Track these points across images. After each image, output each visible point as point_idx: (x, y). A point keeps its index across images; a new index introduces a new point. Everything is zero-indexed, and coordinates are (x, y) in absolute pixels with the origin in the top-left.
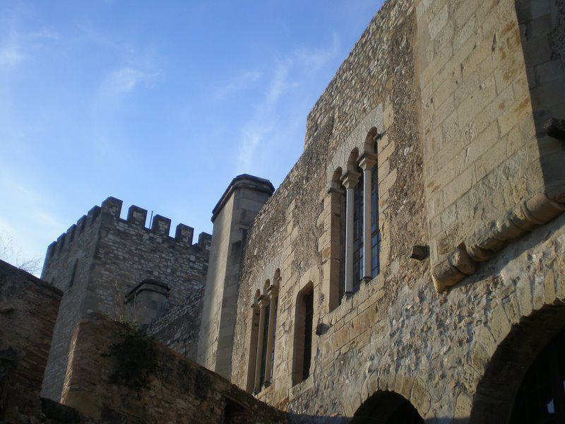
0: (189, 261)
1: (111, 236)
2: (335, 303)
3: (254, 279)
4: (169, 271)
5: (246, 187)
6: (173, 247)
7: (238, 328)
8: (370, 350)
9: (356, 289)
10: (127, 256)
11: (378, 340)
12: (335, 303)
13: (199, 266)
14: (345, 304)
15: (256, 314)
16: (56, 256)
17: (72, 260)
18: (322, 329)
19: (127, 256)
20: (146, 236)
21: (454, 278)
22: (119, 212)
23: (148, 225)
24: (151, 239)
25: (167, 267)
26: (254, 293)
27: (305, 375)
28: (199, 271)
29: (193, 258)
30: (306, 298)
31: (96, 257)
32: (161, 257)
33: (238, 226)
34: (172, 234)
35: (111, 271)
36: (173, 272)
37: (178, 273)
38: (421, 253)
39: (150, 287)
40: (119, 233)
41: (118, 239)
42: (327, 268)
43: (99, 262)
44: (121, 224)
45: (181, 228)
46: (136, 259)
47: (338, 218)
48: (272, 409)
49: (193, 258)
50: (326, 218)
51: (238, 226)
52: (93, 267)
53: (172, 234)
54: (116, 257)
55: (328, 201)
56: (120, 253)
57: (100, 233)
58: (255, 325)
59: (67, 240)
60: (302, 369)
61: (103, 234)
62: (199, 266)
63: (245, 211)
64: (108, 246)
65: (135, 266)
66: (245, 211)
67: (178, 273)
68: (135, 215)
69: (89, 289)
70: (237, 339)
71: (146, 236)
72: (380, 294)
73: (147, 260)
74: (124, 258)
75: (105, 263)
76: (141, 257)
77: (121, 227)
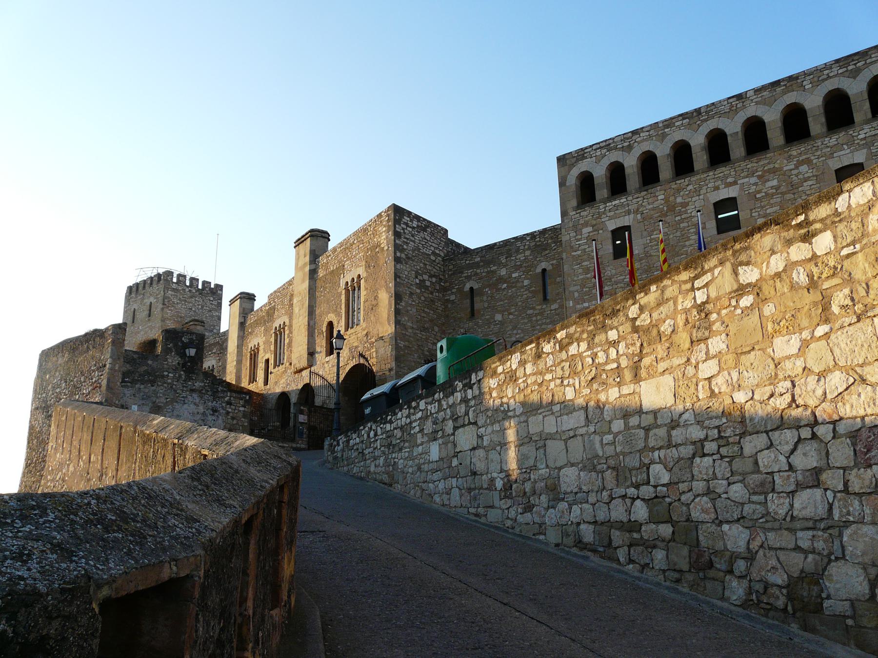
0: (210, 300)
1: (170, 292)
2: (274, 368)
3: (250, 342)
4: (200, 307)
5: (244, 298)
6: (200, 294)
7: (244, 358)
8: (281, 382)
9: (279, 366)
10: (179, 301)
11: (283, 380)
12: (274, 368)
13: (215, 303)
14: (277, 369)
15: (251, 355)
16: (133, 295)
17: (147, 301)
18: (271, 373)
19: (179, 301)
20: (187, 290)
21: (295, 373)
22: (172, 279)
23: (188, 283)
24: (190, 291)
25: (199, 305)
26: (250, 347)
27: (267, 384)
28: (215, 305)
29: (212, 299)
30: (267, 361)
31: (164, 304)
32: (196, 300)
33: (242, 315)
34: (200, 287)
35: (171, 310)
36: (202, 307)
37: (205, 308)
38: (291, 364)
39: (196, 323)
40: (173, 290)
41: (173, 293)
42: (273, 355)
43: (164, 306)
44: (174, 284)
45: (204, 283)
46: (183, 302)
47: (276, 341)
48: (258, 393)
49: (212, 299)
50: (273, 340)
51: (242, 315)
52: (162, 309)
53: (200, 287)
54: (174, 303)
55: (273, 335)
56: (175, 301)
57: (164, 291)
58: (251, 359)
59: (141, 288)
60: (266, 382)
61: (166, 291)
62: (215, 303)
63: (244, 308)
64: (169, 298)
65: (183, 307)
66: (244, 308)
67: (205, 308)
68: (181, 278)
69: (162, 321)
70: (244, 361)
71: (187, 290)
72: (284, 369)
73: (189, 303)
74: (178, 303)
75: (169, 307)
76: (185, 301)
77: (174, 286)
